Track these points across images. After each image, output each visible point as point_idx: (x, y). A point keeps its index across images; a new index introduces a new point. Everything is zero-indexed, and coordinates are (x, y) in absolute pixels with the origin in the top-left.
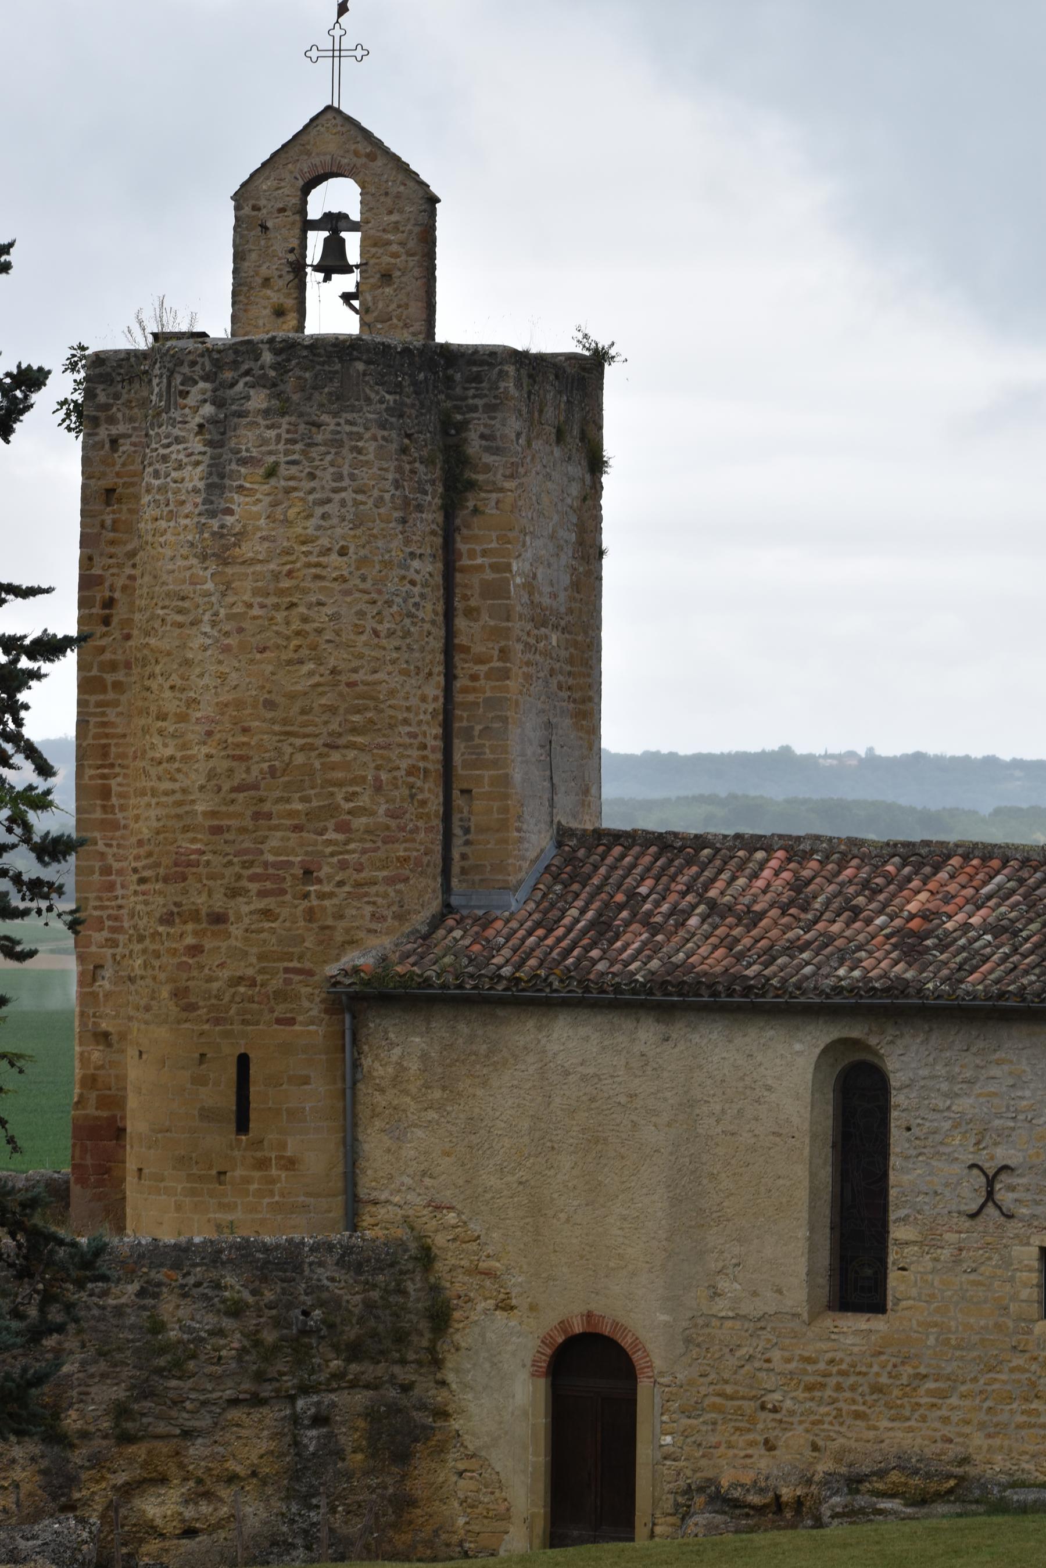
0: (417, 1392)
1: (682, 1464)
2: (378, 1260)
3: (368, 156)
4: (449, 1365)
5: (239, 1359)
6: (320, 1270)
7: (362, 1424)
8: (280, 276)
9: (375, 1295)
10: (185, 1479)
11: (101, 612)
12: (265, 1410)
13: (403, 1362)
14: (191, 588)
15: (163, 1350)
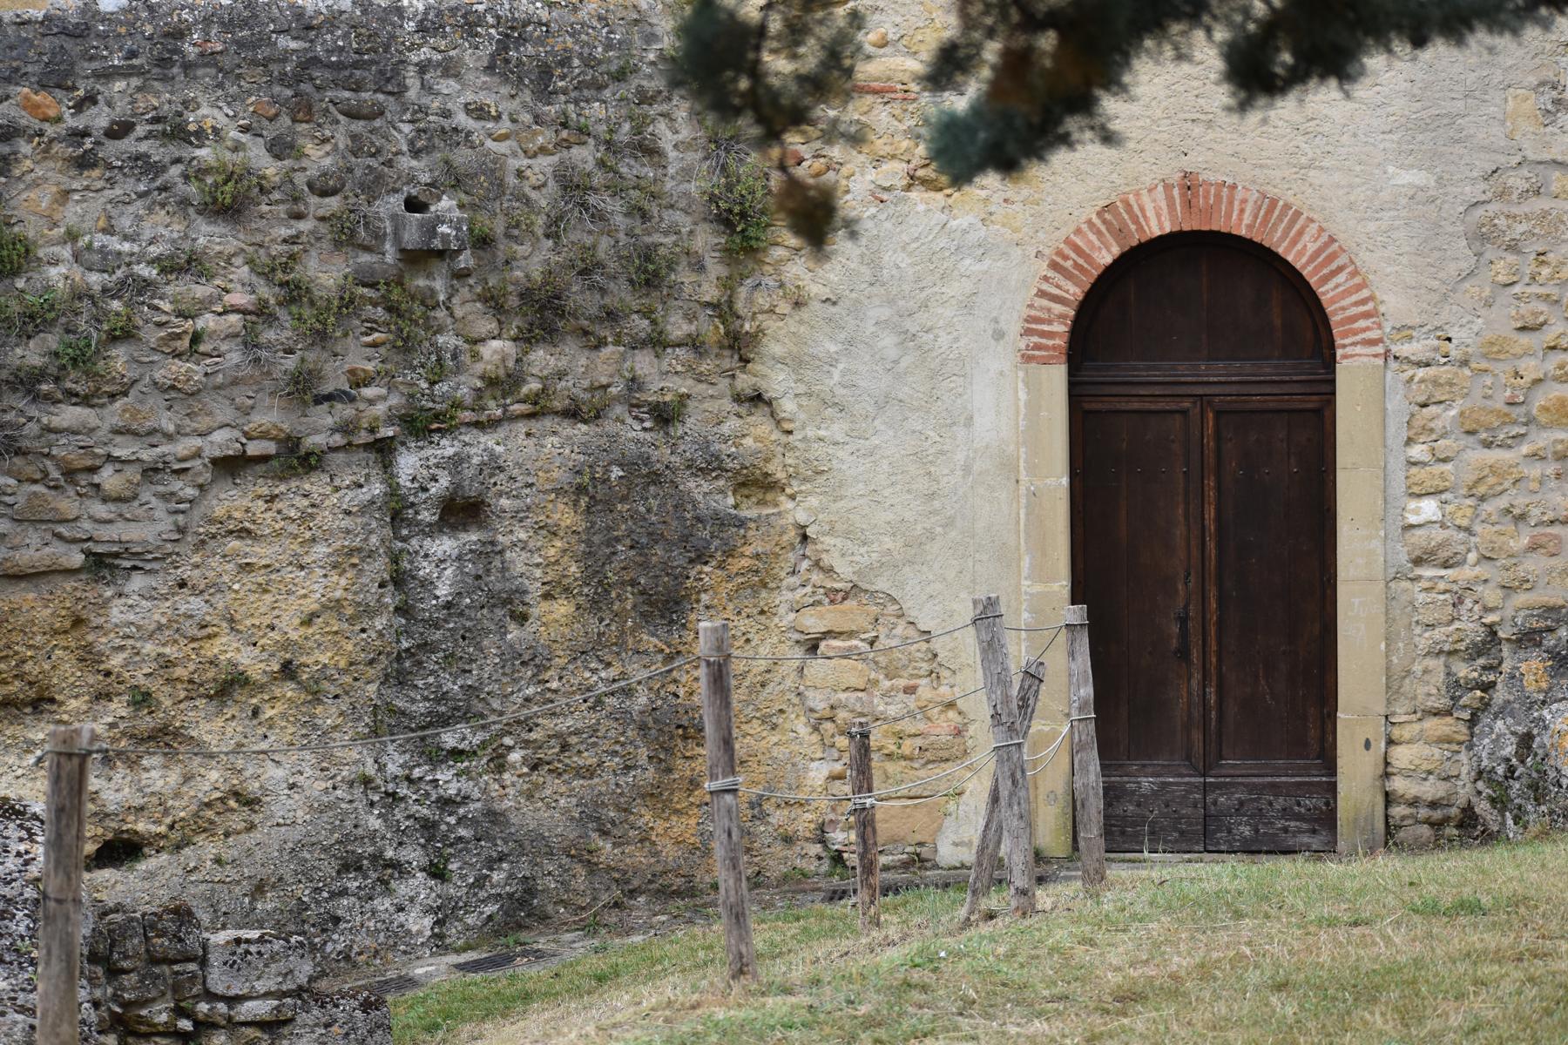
0: (692, 424)
1: (1465, 573)
2: (589, 62)
4: (776, 349)
5: (250, 342)
6: (448, 86)
7: (565, 516)
9: (584, 156)
10: (103, 696)
12: (316, 485)
13: (657, 342)
15: (34, 321)
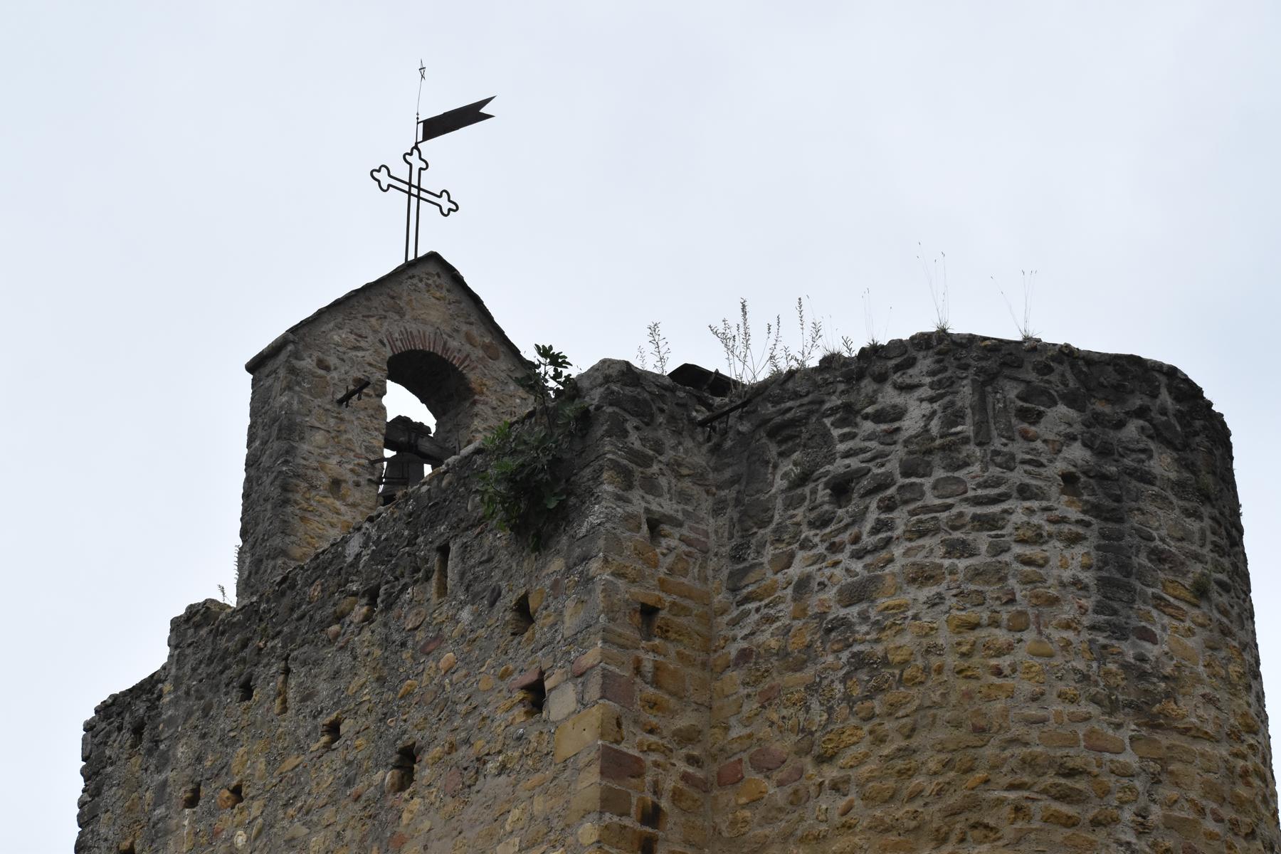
3: (486, 348)
8: (357, 484)
11: (638, 827)
14: (1091, 756)
